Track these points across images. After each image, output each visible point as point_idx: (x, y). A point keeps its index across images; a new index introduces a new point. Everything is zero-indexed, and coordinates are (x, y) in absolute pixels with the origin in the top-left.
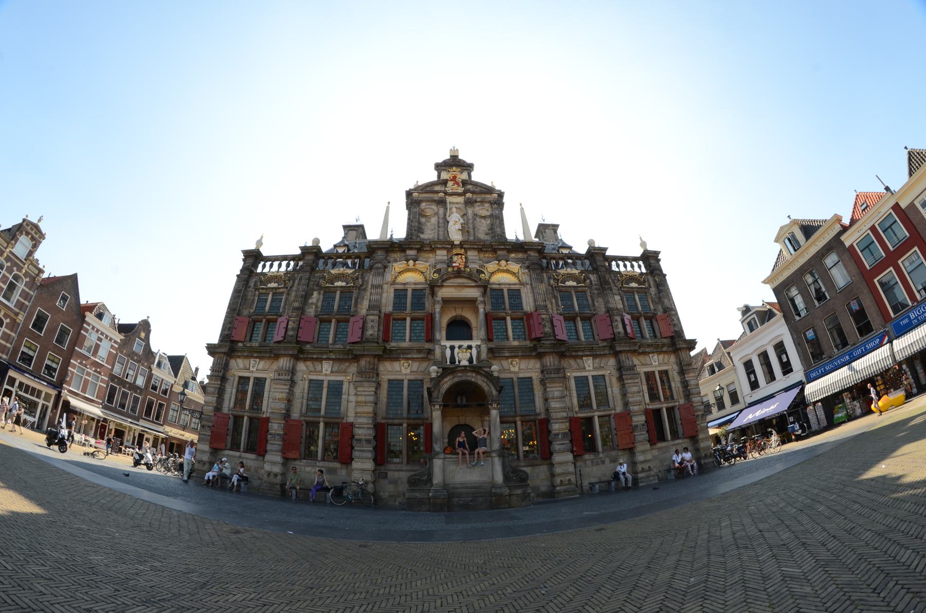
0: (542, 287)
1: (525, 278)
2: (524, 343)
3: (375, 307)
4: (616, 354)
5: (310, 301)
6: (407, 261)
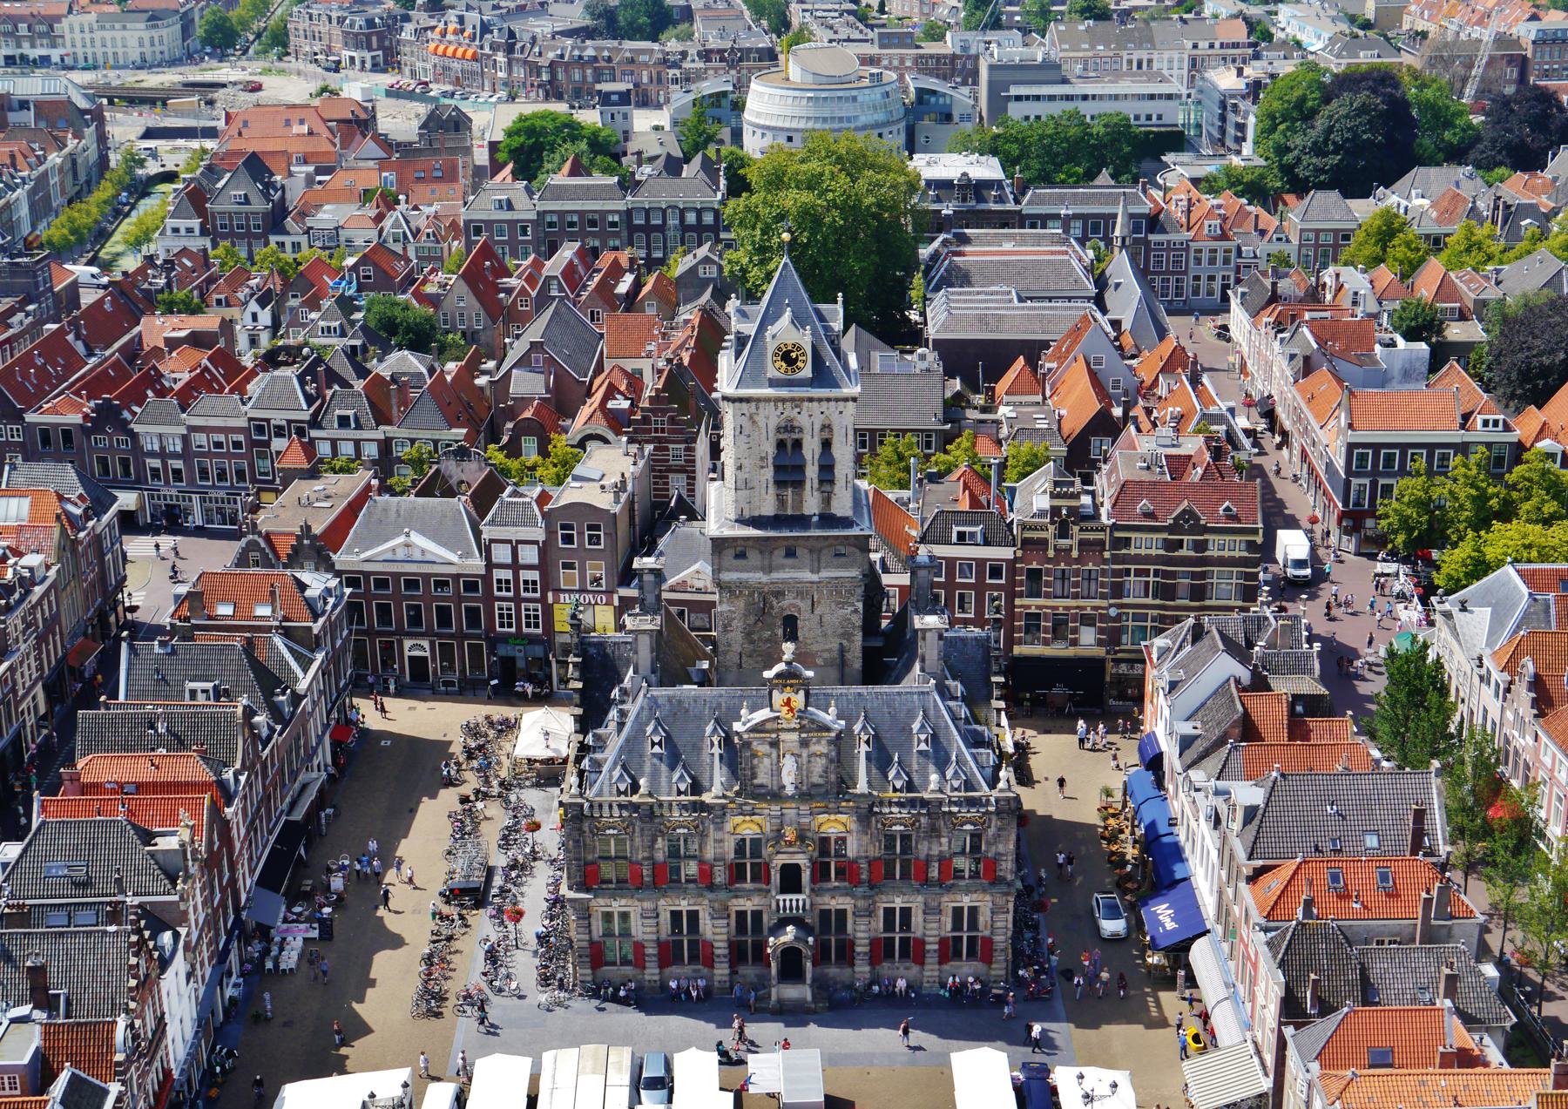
1: (853, 826)
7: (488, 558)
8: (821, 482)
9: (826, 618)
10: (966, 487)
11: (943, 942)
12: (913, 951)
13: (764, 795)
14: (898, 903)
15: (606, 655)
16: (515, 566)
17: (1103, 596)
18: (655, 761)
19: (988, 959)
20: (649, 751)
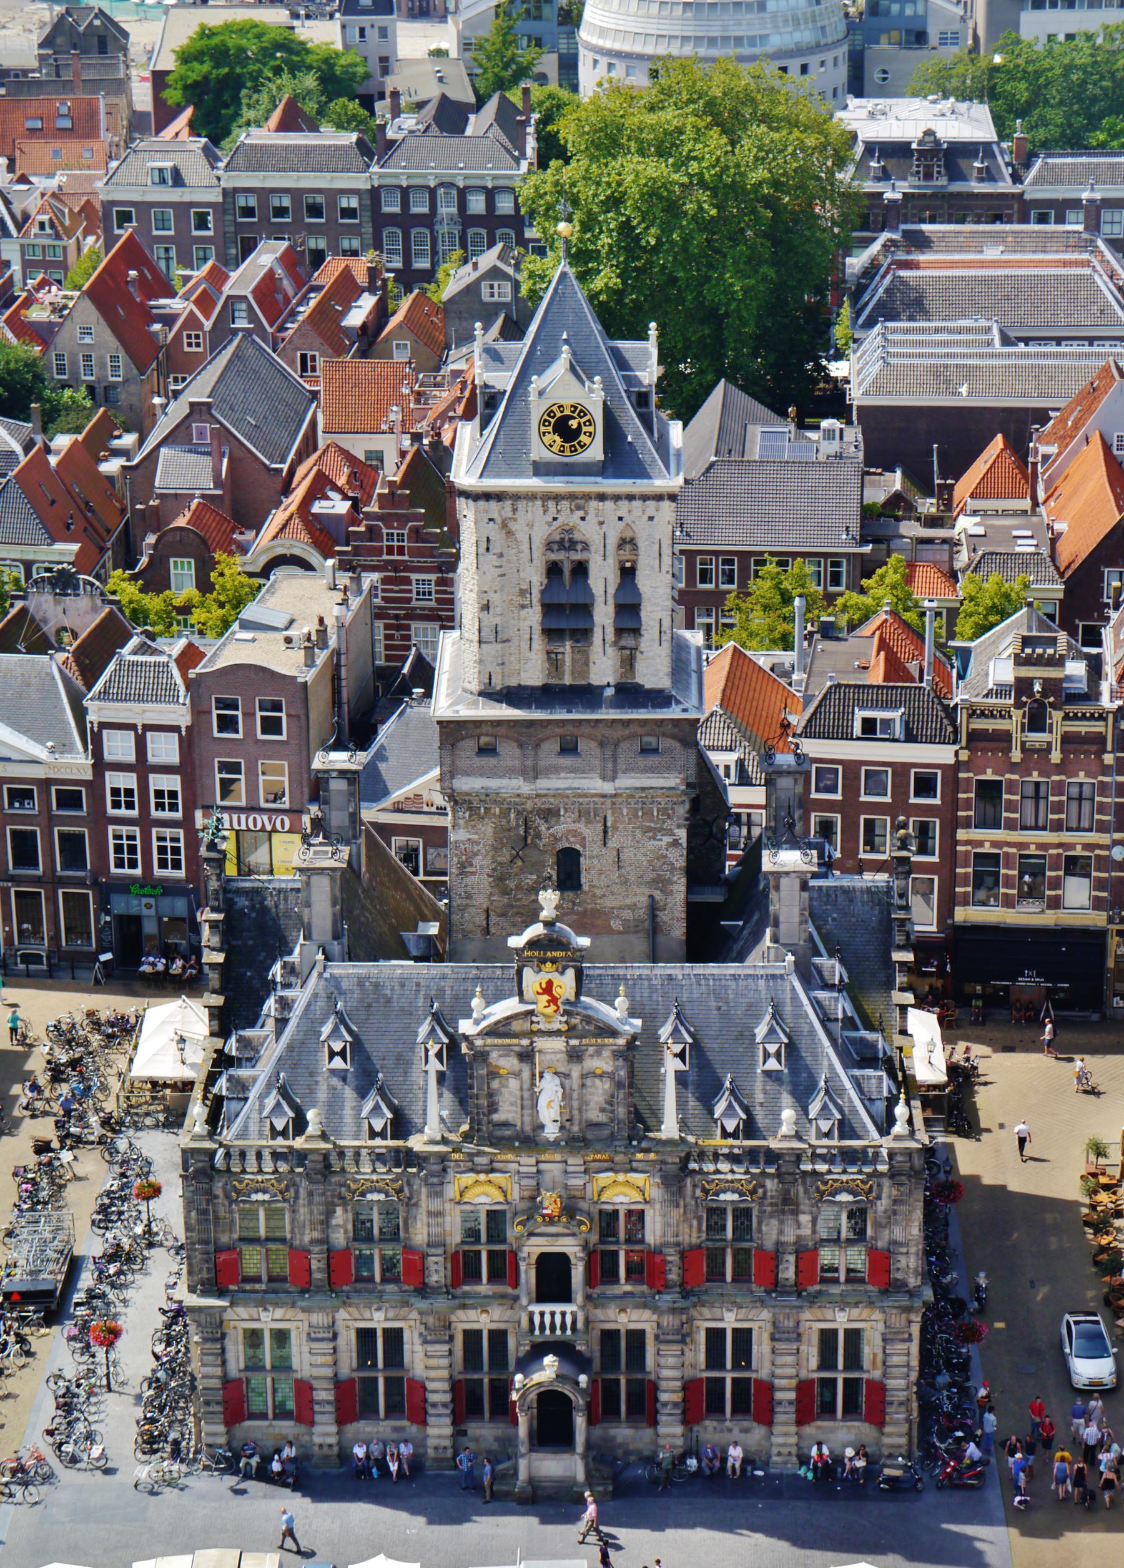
1: (655, 1192)
5: (334, 1222)
7: (98, 754)
8: (619, 632)
9: (627, 855)
10: (883, 645)
11: (804, 1387)
12: (754, 1401)
13: (511, 1139)
14: (730, 1321)
15: (264, 910)
16: (142, 767)
17: (1102, 828)
18: (335, 1081)
19: (877, 1417)
20: (325, 1065)
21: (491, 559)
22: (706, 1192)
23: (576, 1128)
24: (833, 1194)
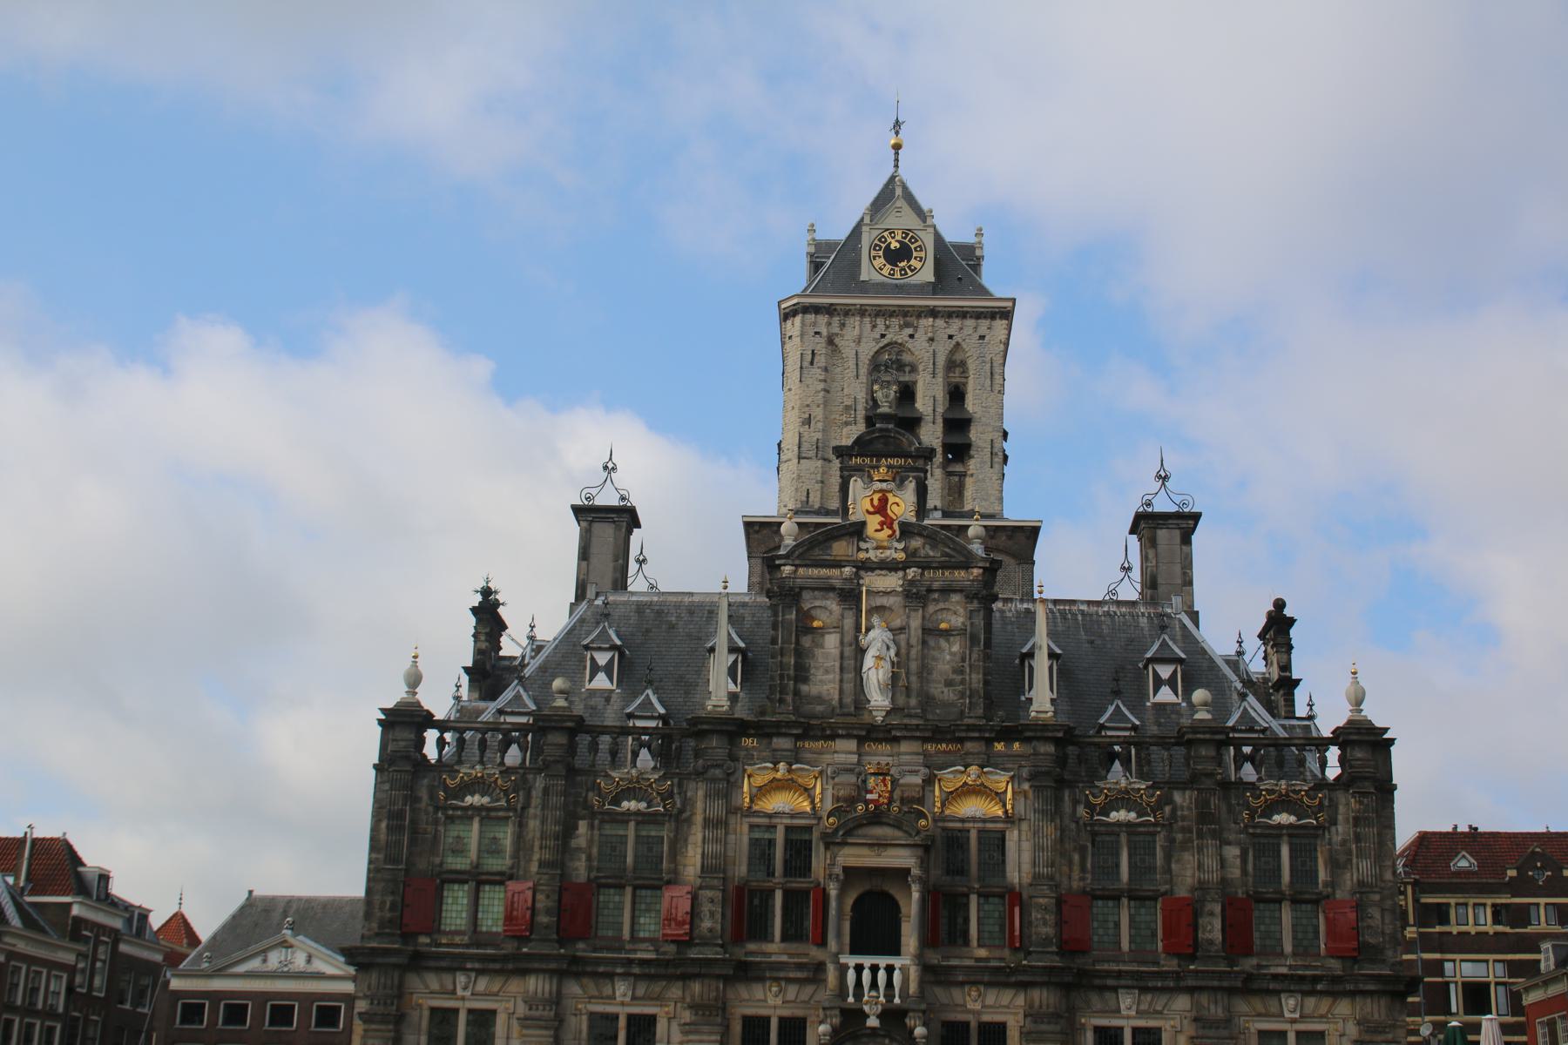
0: (1049, 831)
2: (997, 953)
3: (713, 868)
4: (1191, 990)
5: (574, 843)
6: (775, 763)
21: (817, 372)
22: (1091, 807)
23: (913, 702)
24: (1270, 809)
